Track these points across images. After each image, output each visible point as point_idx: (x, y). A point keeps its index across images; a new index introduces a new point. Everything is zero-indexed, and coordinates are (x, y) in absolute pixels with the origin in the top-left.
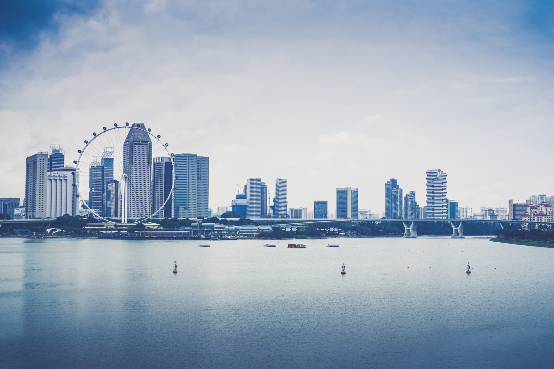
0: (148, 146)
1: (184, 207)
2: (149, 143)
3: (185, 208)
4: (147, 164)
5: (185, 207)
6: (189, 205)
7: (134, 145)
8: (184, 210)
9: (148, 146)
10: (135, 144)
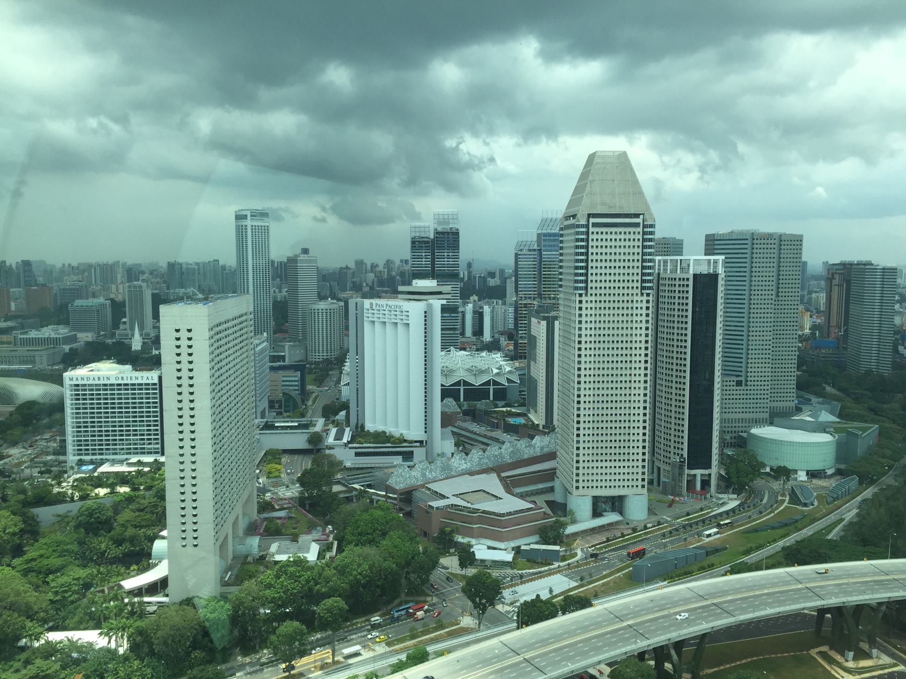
0: (640, 229)
1: (736, 379)
3: (739, 383)
4: (635, 291)
5: (739, 379)
7: (591, 230)
8: (735, 388)
9: (640, 229)
10: (595, 225)
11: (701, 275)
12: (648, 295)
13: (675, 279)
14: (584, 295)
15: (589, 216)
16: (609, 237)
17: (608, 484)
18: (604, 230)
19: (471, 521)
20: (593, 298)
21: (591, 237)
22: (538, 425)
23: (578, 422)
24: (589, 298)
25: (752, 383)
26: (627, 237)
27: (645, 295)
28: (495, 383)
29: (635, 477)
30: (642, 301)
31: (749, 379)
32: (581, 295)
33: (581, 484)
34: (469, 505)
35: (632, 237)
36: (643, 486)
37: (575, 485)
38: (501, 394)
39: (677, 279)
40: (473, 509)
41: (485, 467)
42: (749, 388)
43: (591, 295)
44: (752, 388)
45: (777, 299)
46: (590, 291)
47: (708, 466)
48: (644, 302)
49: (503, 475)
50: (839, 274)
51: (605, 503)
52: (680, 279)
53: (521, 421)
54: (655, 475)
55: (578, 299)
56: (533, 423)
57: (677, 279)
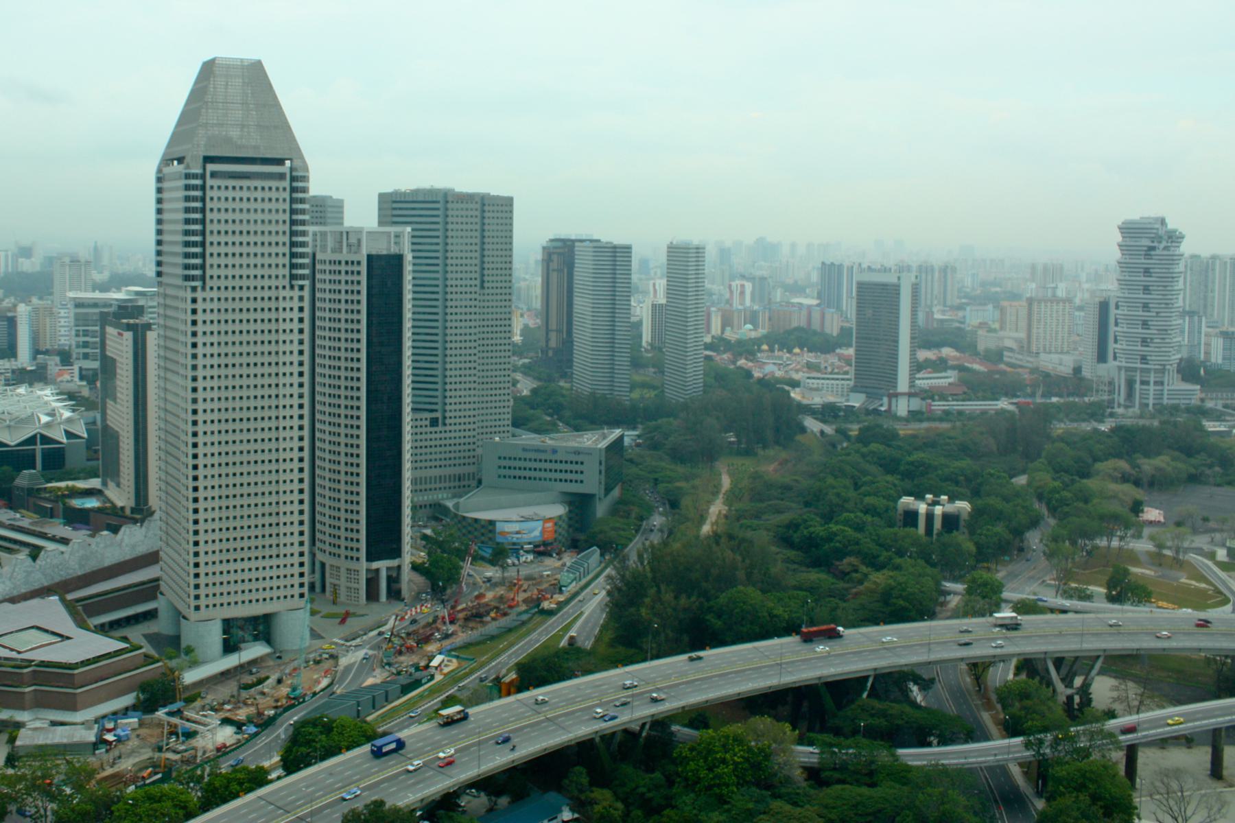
2: (292, 169)
3: (434, 422)
5: (434, 415)
6: (448, 407)
7: (209, 182)
8: (429, 429)
9: (286, 184)
10: (214, 175)
11: (379, 257)
12: (301, 288)
13: (340, 262)
14: (199, 289)
15: (208, 159)
16: (238, 194)
17: (247, 597)
18: (231, 183)
19: (20, 681)
20: (215, 294)
21: (209, 194)
22: (123, 508)
23: (196, 500)
24: (208, 294)
25: (453, 421)
26: (267, 195)
27: (296, 288)
28: (45, 440)
29: (288, 582)
30: (291, 298)
31: (448, 414)
32: (194, 289)
33: (202, 602)
34: (14, 655)
35: (274, 195)
36: (302, 595)
37: (193, 603)
38: (55, 460)
39: (343, 263)
40: (23, 660)
41: (36, 586)
42: (448, 428)
43: (212, 288)
44: (453, 428)
45: (482, 292)
46: (209, 283)
47: (396, 553)
48: (296, 299)
49: (70, 597)
50: (559, 254)
51: (242, 628)
52: (347, 263)
53: (91, 503)
54: (318, 575)
55: (189, 295)
56: (114, 506)
57: (343, 263)
